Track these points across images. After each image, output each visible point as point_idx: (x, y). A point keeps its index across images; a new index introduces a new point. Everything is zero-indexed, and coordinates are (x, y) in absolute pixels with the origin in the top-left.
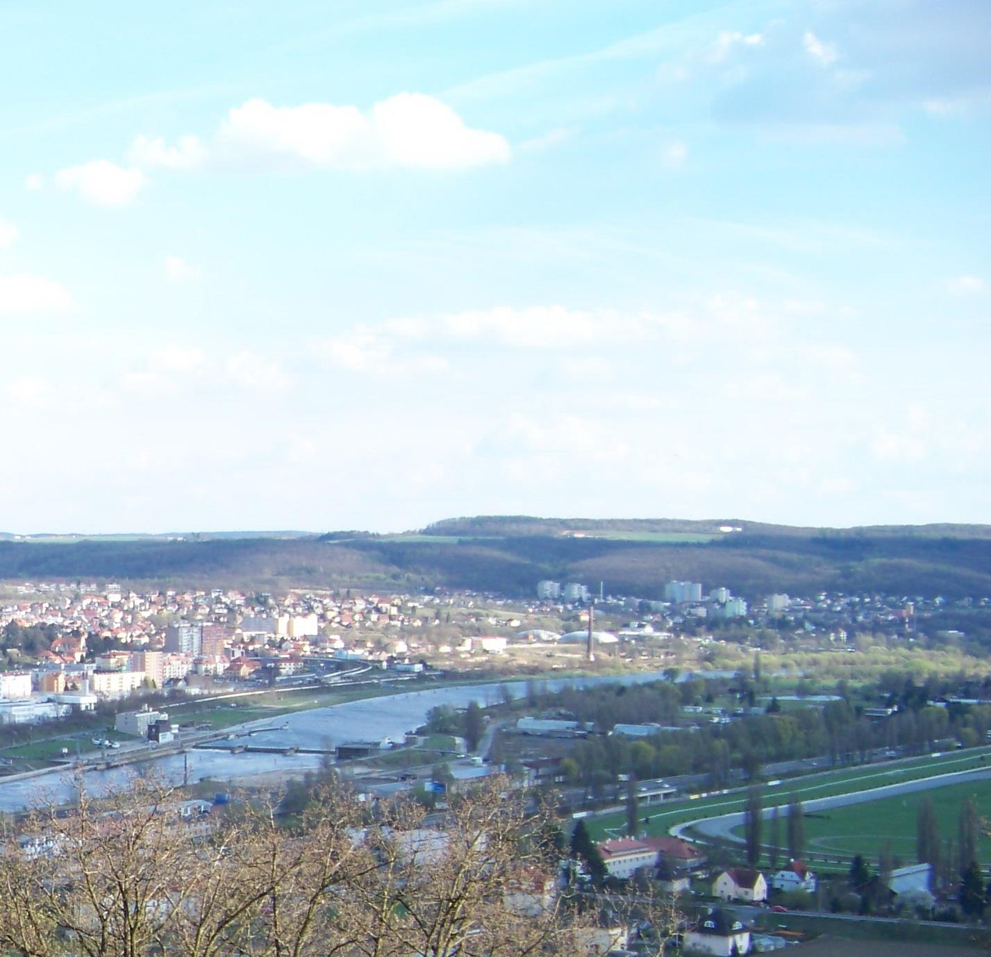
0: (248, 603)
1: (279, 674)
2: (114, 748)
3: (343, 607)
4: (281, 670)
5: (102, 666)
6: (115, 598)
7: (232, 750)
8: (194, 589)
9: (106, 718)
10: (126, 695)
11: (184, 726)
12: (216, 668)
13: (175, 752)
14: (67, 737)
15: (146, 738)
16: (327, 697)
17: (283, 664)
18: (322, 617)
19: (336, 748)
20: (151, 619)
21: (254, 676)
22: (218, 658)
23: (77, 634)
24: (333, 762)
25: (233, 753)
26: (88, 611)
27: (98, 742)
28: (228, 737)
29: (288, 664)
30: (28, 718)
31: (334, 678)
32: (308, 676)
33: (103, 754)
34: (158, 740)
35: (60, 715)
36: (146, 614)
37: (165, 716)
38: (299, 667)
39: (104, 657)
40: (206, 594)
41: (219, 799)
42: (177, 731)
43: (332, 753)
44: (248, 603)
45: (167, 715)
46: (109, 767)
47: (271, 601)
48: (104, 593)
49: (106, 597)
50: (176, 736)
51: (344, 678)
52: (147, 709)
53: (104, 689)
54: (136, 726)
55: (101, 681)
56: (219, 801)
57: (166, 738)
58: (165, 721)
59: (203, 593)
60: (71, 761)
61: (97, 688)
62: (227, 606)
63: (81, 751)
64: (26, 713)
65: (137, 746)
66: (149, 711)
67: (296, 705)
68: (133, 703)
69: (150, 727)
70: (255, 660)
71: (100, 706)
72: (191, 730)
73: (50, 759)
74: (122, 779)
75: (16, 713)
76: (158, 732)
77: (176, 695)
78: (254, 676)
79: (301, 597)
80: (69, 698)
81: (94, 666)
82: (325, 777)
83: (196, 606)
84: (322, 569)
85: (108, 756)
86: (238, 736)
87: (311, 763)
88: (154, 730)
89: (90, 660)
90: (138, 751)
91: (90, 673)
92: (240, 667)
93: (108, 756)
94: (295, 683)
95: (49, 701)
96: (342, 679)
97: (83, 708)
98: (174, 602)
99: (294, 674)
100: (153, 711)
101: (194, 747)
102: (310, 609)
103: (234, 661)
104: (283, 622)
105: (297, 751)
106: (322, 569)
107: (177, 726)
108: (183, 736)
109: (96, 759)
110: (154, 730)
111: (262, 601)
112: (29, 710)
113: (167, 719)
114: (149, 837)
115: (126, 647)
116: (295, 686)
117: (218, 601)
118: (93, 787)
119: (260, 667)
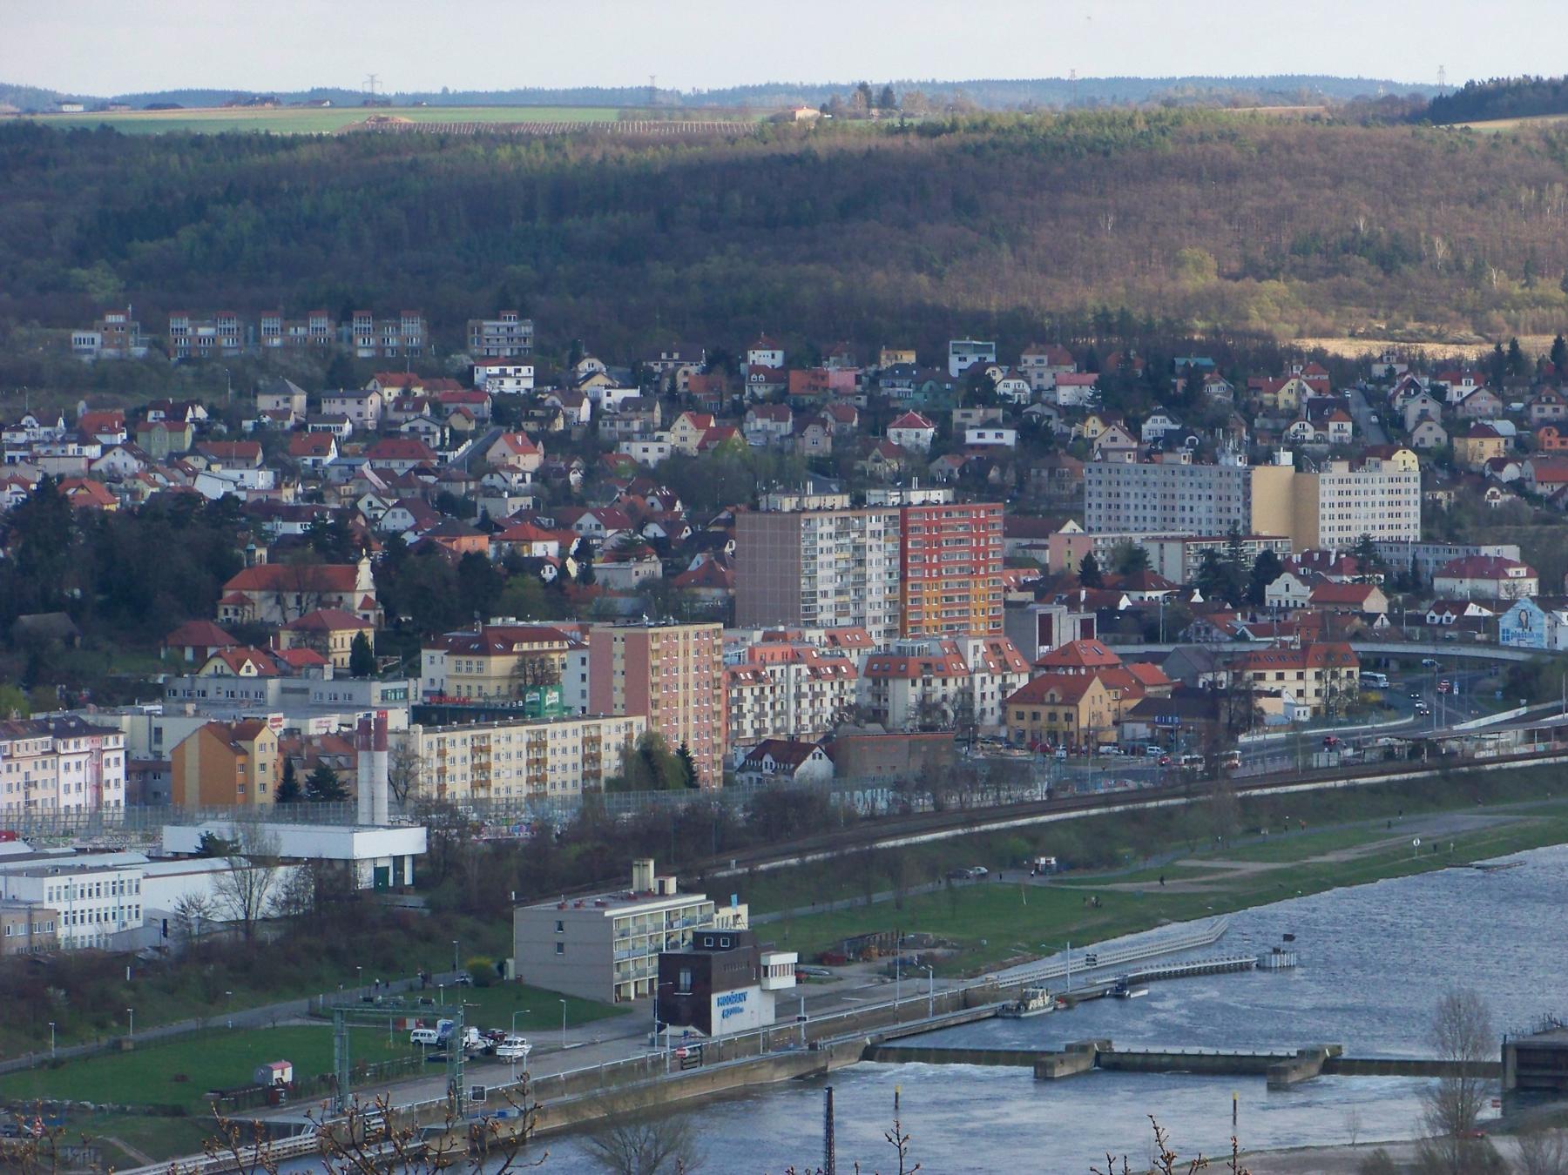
1: (1254, 720)
2: (504, 1062)
3: (1535, 413)
4: (1263, 703)
5: (451, 691)
7: (1042, 1067)
10: (562, 818)
11: (821, 959)
12: (967, 694)
13: (782, 1076)
14: (289, 1013)
15: (649, 1014)
17: (1271, 675)
19: (1505, 1048)
21: (1142, 730)
22: (975, 651)
24: (1489, 1112)
25: (1044, 1076)
27: (433, 1035)
28: (1023, 1003)
29: (1291, 674)
30: (112, 927)
32: (1385, 730)
33: (453, 1089)
34: (706, 1027)
35: (257, 915)
36: (650, 453)
37: (735, 916)
38: (1341, 686)
39: (458, 649)
40: (922, 362)
42: (789, 982)
43: (1488, 1070)
45: (743, 910)
47: (1217, 390)
48: (464, 360)
49: (467, 377)
50: (785, 1005)
51: (1544, 735)
52: (653, 884)
53: (459, 788)
54: (609, 964)
55: (448, 761)
57: (742, 1013)
58: (735, 938)
59: (909, 358)
61: (426, 786)
62: (1015, 414)
63: (356, 1077)
64: (107, 903)
65: (604, 1051)
66: (662, 894)
67: (1330, 858)
68: (584, 854)
69: (668, 965)
70: (1142, 658)
71: (437, 865)
72: (853, 974)
75: (62, 906)
76: (703, 987)
77: (785, 815)
78: (1142, 730)
80: (302, 839)
81: (416, 688)
83: (879, 416)
84: (1441, 251)
85: (479, 1094)
86: (1068, 1001)
88: (685, 978)
89: (395, 660)
90: (615, 1071)
91: (398, 718)
92: (1073, 694)
93: (479, 1094)
94: (1321, 759)
95: (210, 848)
96: (1530, 737)
97: (366, 877)
98: (775, 404)
99: (1318, 717)
100: (683, 890)
101: (868, 1054)
102: (1394, 432)
103: (1046, 664)
105: (1334, 1065)
106: (1441, 251)
107: (792, 958)
108: (814, 1002)
109: (424, 1111)
110: (685, 978)
112: (118, 888)
113: (743, 925)
116: (1328, 773)
117: (978, 390)
119: (1166, 691)
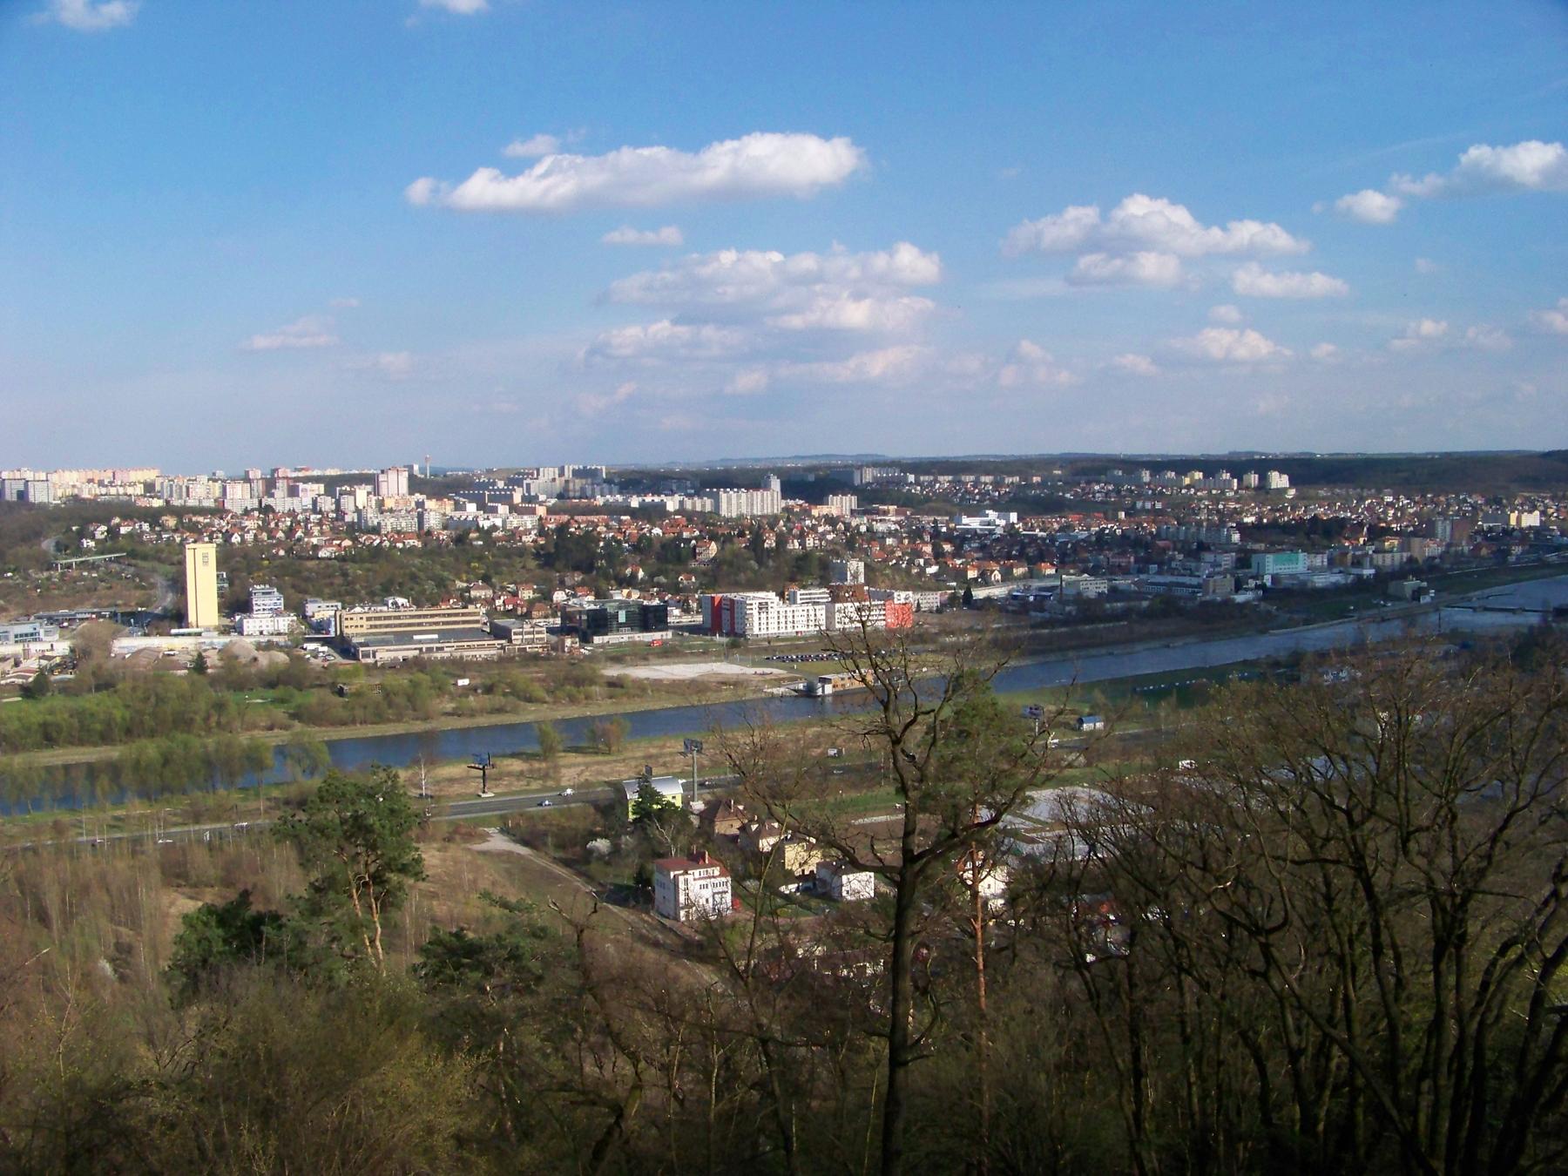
0: (1487, 503)
6: (1389, 499)
7: (1474, 609)
8: (1447, 493)
9: (1385, 579)
16: (1546, 571)
18: (1543, 513)
20: (1415, 514)
23: (1361, 524)
26: (1369, 508)
31: (1552, 557)
32: (1533, 556)
37: (1425, 584)
41: (1466, 645)
44: (1487, 503)
46: (1383, 620)
56: (1464, 646)
57: (1425, 600)
60: (1356, 615)
65: (1404, 605)
68: (1400, 573)
72: (1444, 594)
73: (1342, 614)
74: (1395, 629)
79: (1528, 499)
80: (1355, 571)
82: (1545, 629)
83: (1449, 505)
87: (1534, 619)
98: (1432, 501)
104: (1513, 517)
111: (1498, 501)
114: (1416, 669)
115: (1397, 534)
117: (1465, 501)
118: (1373, 634)
